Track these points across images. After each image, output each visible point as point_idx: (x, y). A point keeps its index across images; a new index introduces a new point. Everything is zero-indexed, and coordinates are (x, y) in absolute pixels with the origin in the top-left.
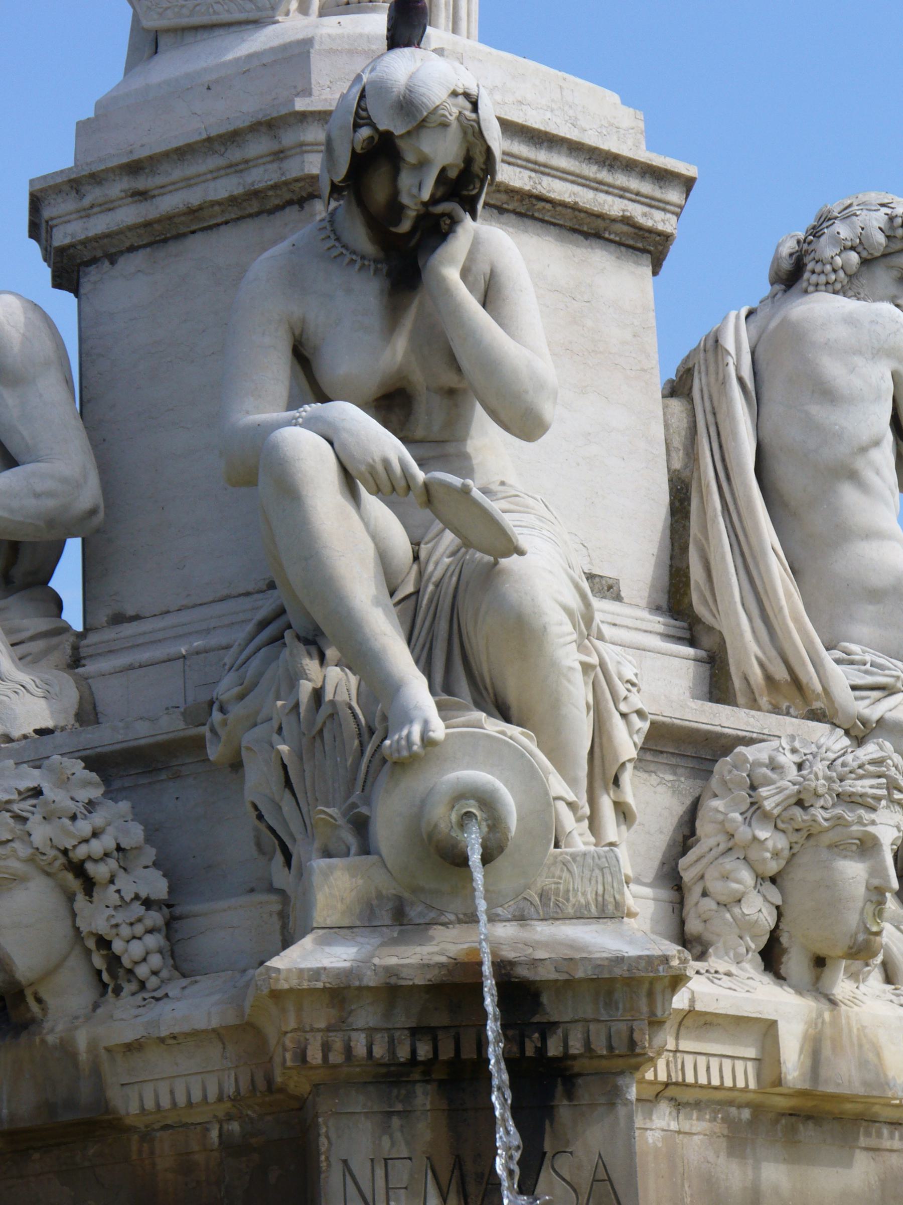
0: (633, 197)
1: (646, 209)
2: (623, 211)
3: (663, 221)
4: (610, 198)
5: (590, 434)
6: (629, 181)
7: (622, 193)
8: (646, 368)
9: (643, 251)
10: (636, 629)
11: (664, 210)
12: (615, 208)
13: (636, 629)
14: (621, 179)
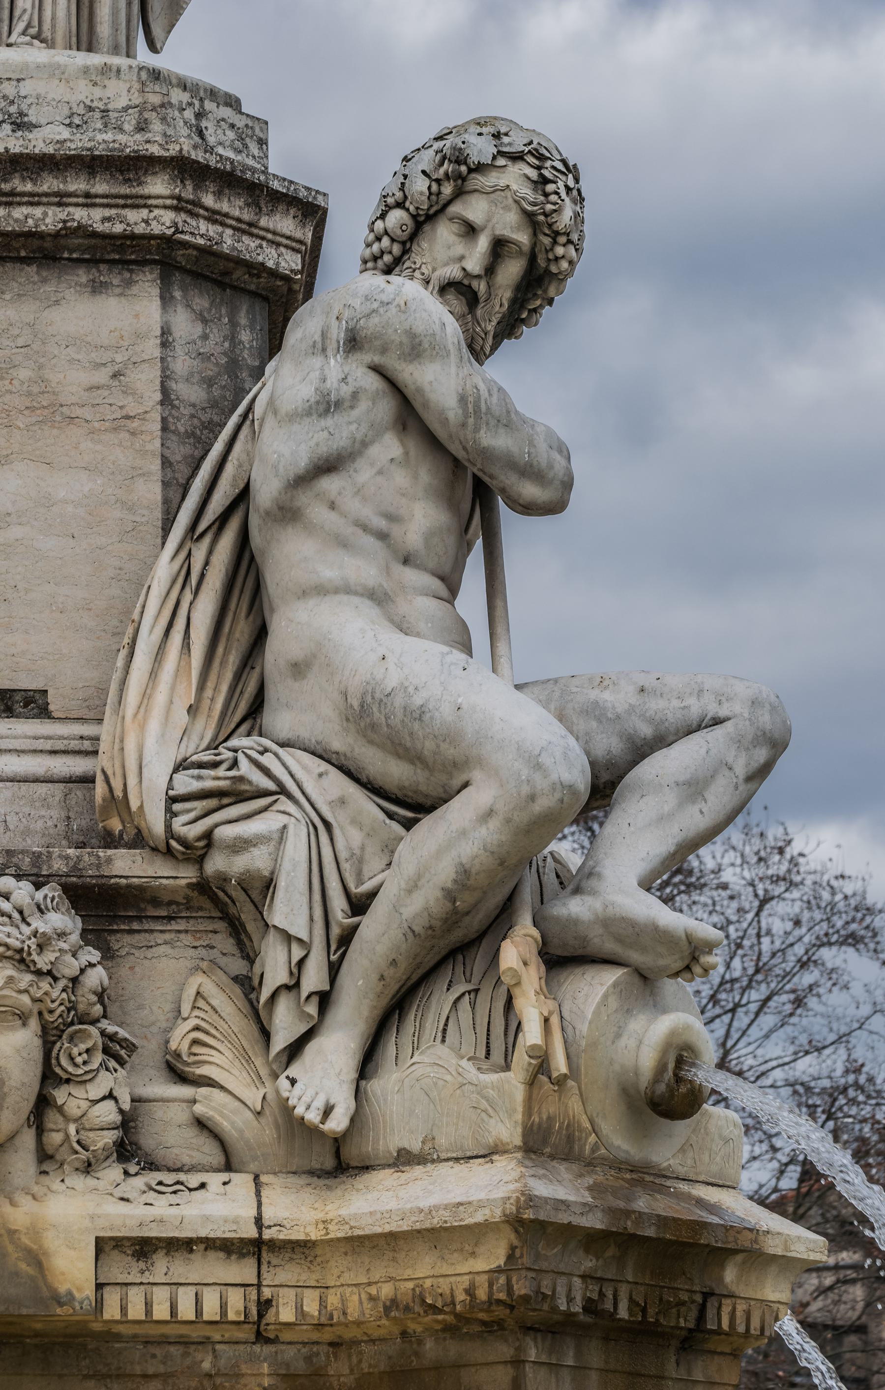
0: (80, 200)
1: (108, 212)
2: (65, 222)
3: (146, 222)
4: (38, 212)
5: (9, 514)
6: (65, 182)
7: (61, 199)
8: (132, 414)
9: (142, 263)
10: (35, 751)
11: (145, 206)
12: (48, 221)
13: (35, 751)
14: (49, 184)
